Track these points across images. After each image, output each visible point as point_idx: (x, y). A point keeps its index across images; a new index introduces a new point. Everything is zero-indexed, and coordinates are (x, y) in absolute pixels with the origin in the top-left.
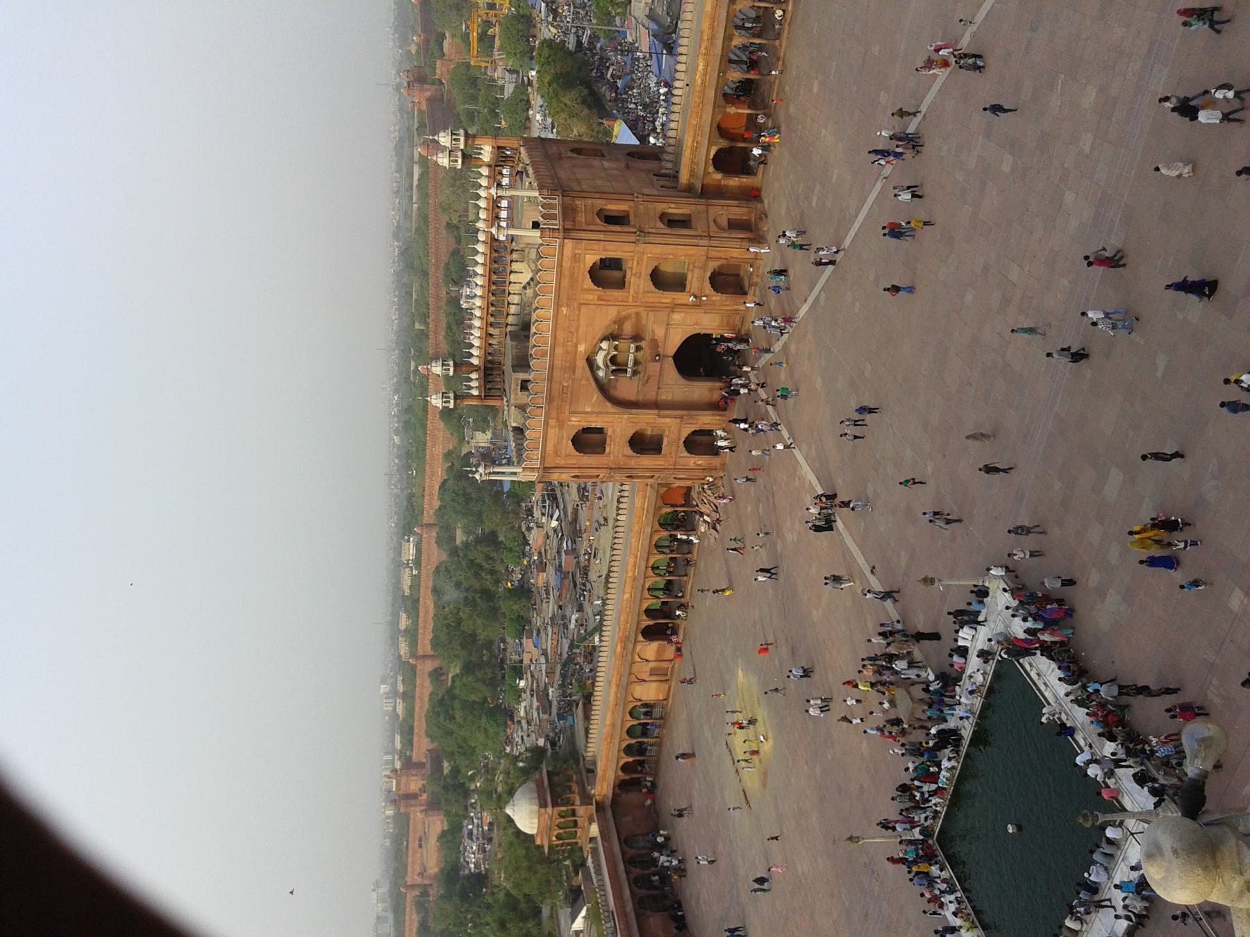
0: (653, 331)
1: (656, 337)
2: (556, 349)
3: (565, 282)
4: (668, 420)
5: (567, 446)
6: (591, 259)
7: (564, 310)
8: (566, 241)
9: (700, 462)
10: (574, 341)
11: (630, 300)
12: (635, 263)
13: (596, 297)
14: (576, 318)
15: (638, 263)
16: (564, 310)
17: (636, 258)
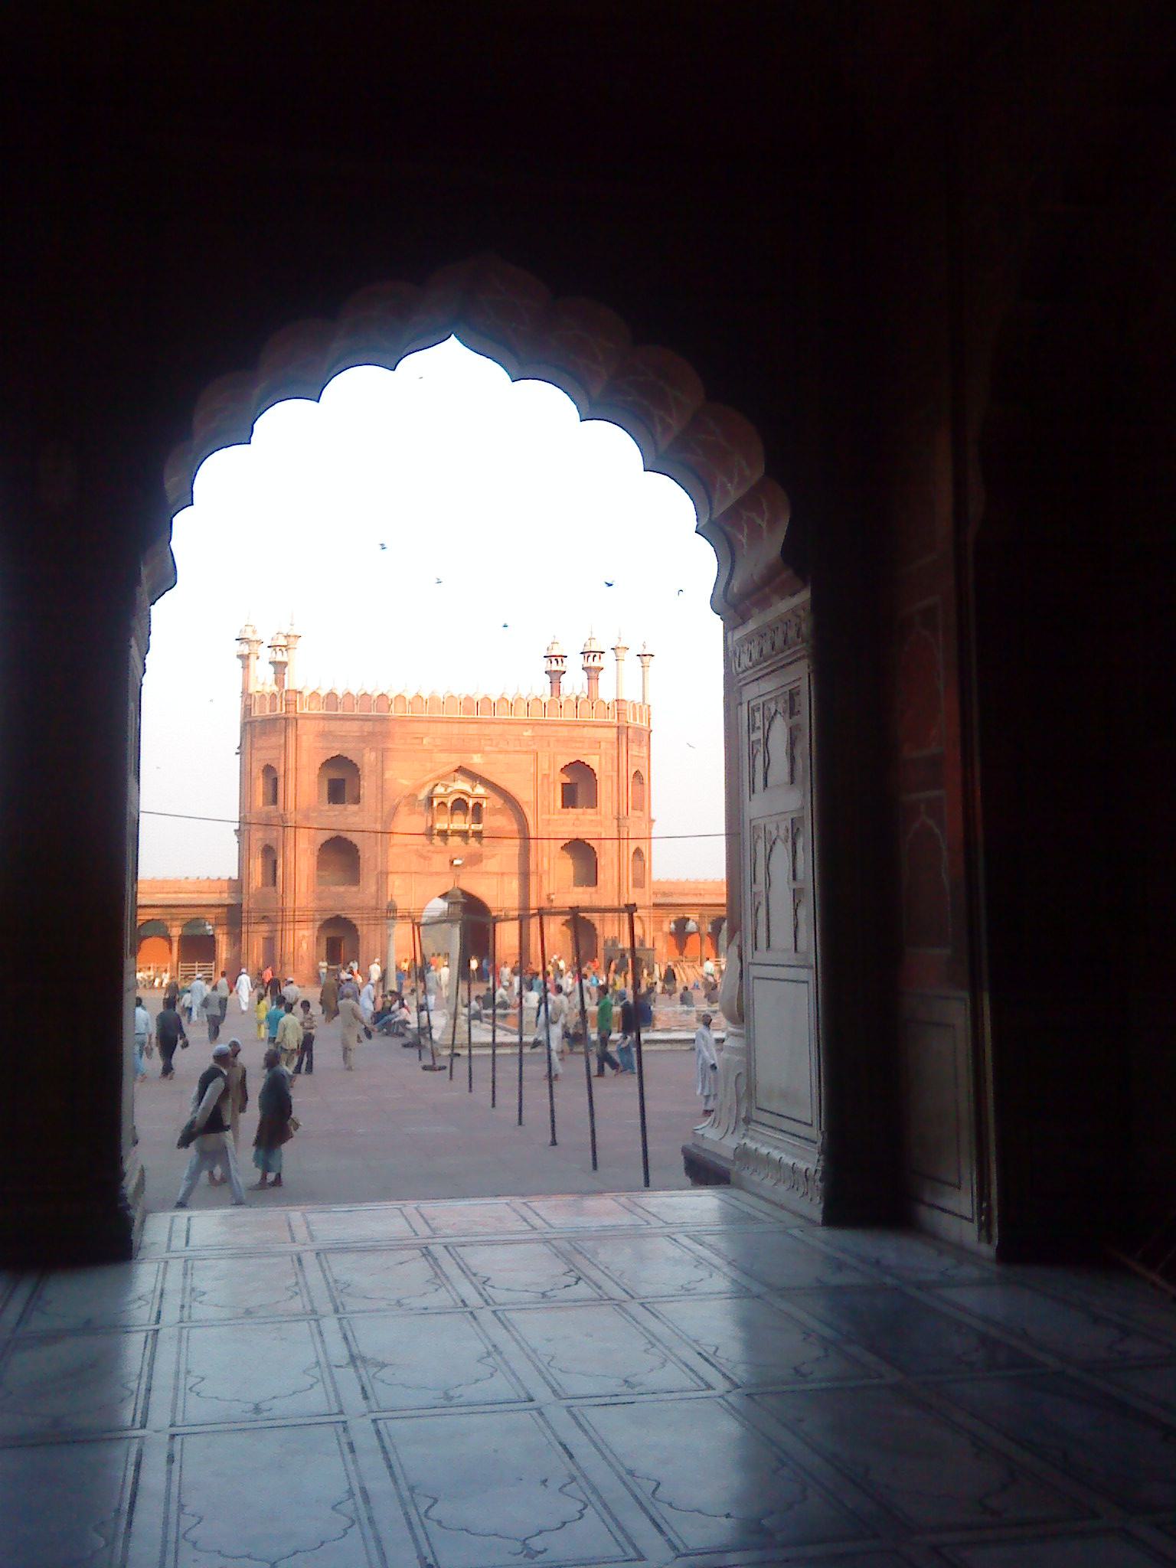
0: (493, 856)
1: (484, 861)
2: (475, 726)
3: (564, 732)
4: (373, 889)
5: (332, 748)
6: (593, 761)
7: (528, 733)
8: (615, 730)
9: (304, 946)
10: (487, 748)
11: (547, 817)
12: (593, 818)
13: (546, 772)
14: (518, 748)
15: (592, 821)
16: (528, 733)
17: (599, 818)
